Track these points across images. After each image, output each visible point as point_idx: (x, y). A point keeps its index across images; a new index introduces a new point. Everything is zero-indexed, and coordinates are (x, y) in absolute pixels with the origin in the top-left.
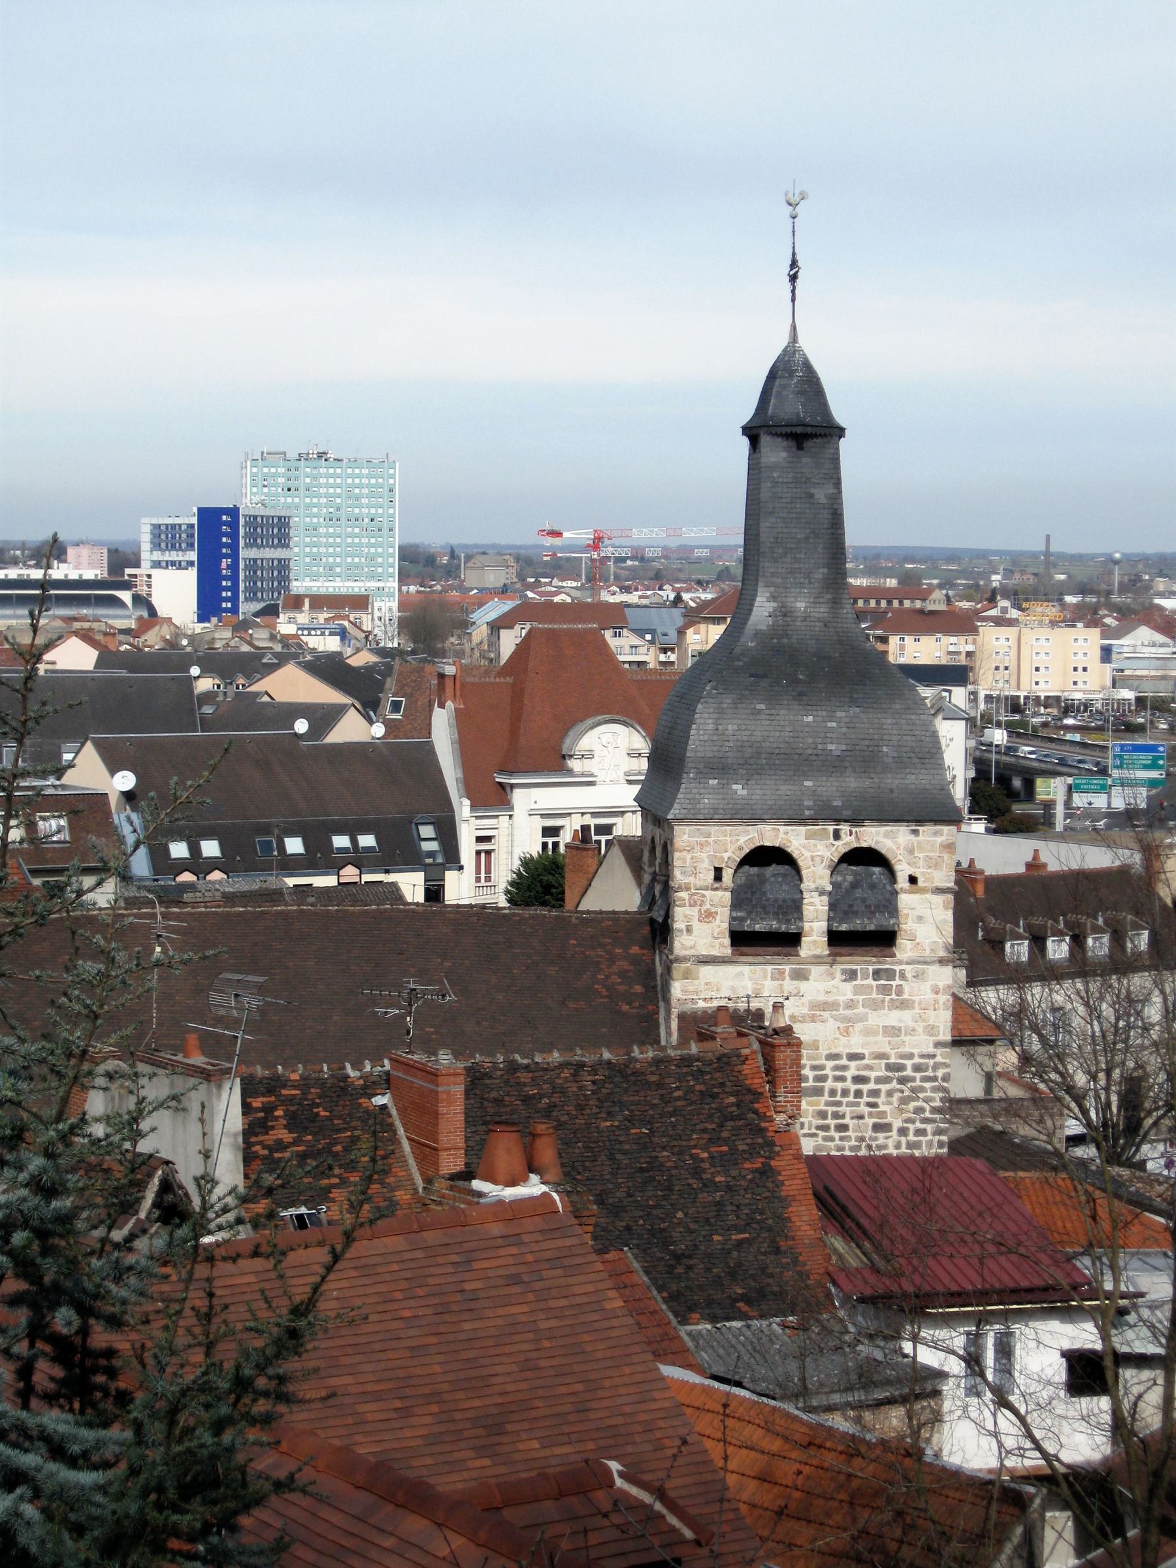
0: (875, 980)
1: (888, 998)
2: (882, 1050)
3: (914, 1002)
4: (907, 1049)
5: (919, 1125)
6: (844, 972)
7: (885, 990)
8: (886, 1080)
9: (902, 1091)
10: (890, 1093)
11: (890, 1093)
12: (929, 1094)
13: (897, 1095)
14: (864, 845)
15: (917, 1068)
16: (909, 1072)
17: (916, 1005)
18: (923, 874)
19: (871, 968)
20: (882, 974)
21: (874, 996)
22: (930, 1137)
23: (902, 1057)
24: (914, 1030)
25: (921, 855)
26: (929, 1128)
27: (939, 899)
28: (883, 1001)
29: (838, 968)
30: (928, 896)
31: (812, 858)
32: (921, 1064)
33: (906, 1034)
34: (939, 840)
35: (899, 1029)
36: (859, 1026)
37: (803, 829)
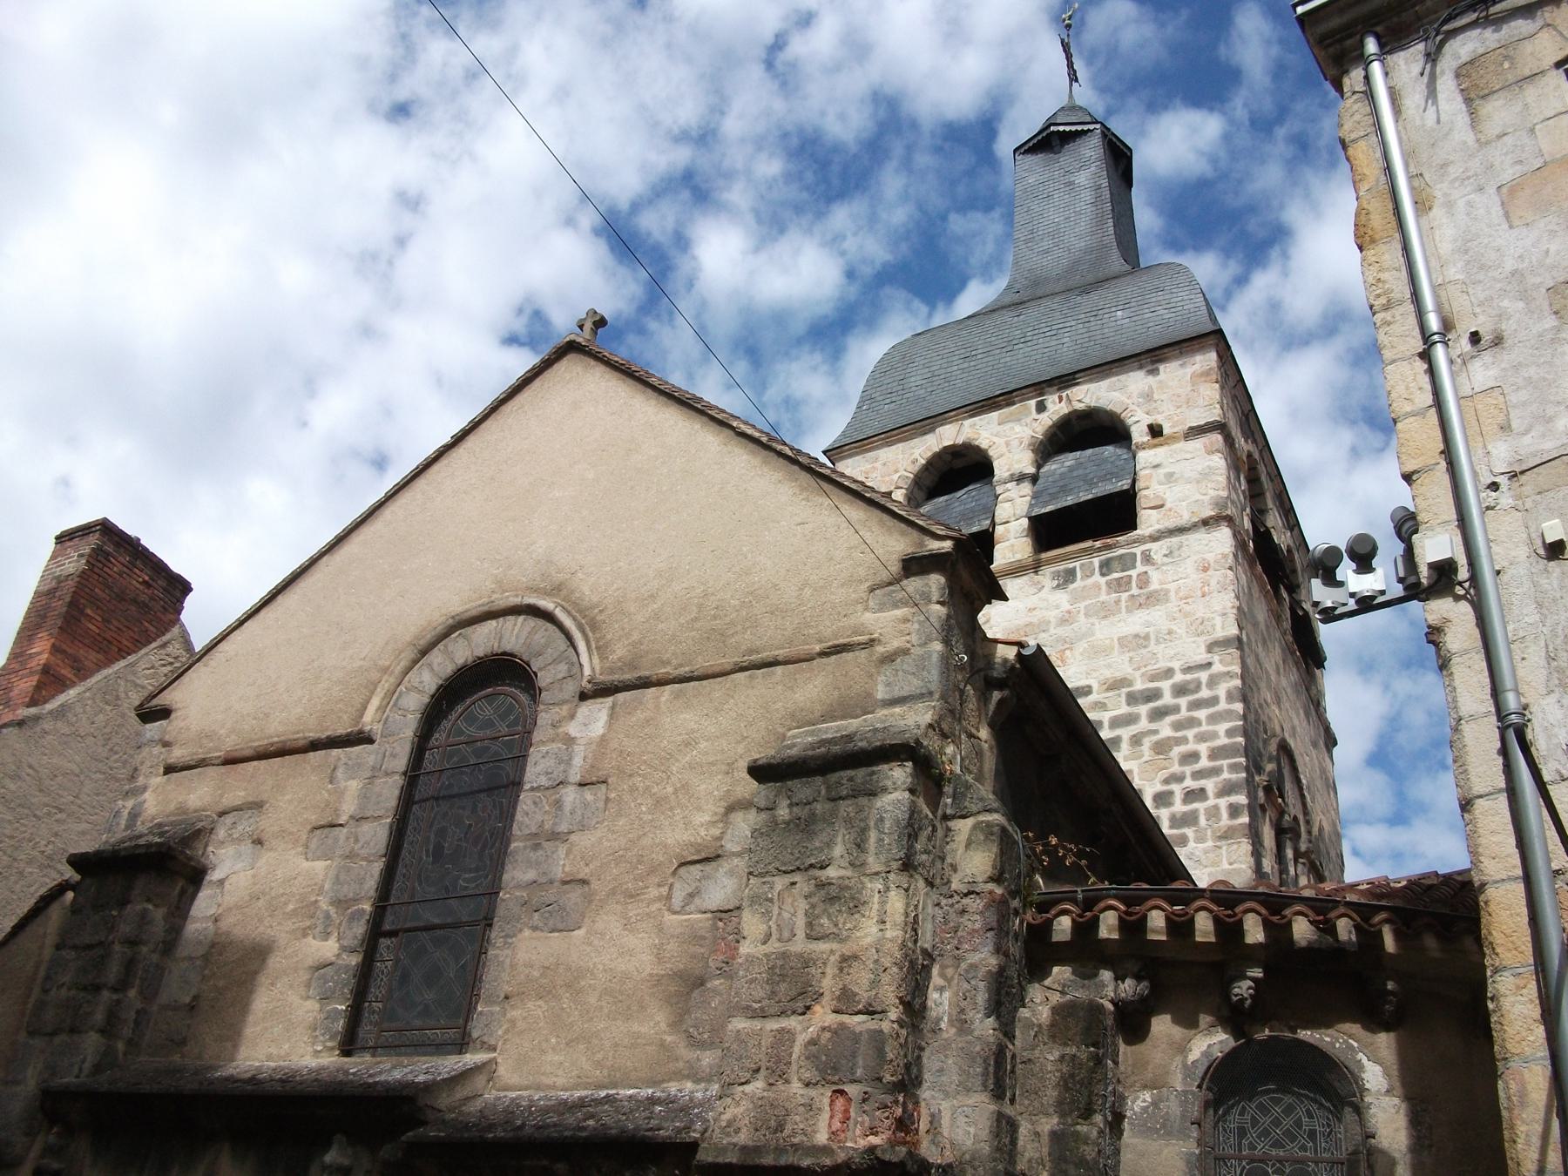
0: (1103, 575)
1: (1125, 596)
2: (1119, 675)
3: (1167, 592)
4: (1163, 664)
5: (1189, 783)
6: (1056, 575)
7: (1121, 585)
8: (1130, 720)
9: (1156, 732)
10: (1136, 741)
11: (1136, 741)
12: (1205, 728)
13: (1147, 742)
14: (1079, 406)
15: (1180, 690)
16: (1167, 699)
17: (1172, 594)
18: (1169, 418)
19: (1096, 561)
20: (1115, 564)
21: (1104, 597)
22: (1211, 802)
23: (1153, 678)
24: (1170, 633)
25: (1164, 397)
26: (1210, 785)
27: (1198, 444)
28: (1118, 602)
29: (1048, 571)
30: (1182, 445)
31: (1007, 444)
32: (1188, 682)
33: (1158, 642)
34: (1189, 370)
35: (1147, 637)
36: (1082, 645)
37: (995, 415)
